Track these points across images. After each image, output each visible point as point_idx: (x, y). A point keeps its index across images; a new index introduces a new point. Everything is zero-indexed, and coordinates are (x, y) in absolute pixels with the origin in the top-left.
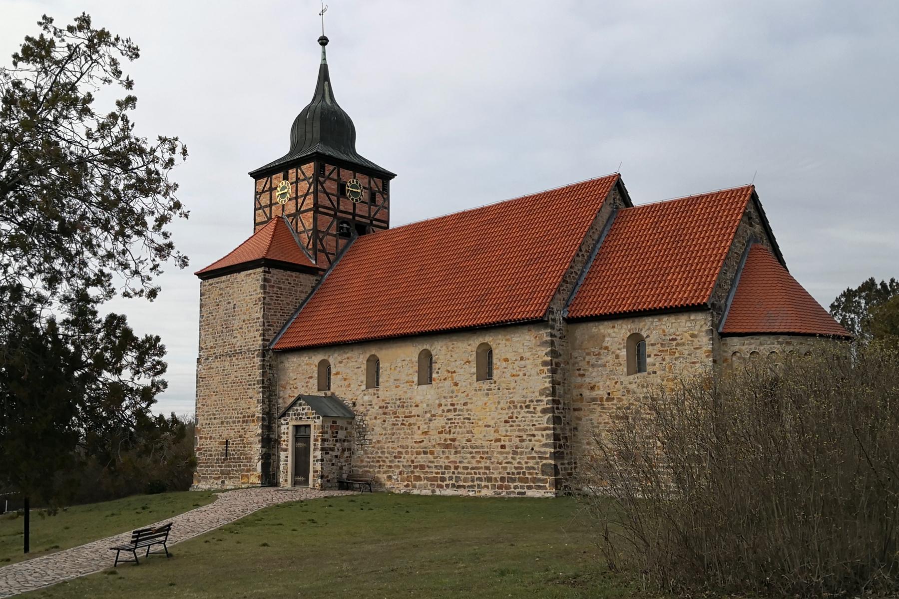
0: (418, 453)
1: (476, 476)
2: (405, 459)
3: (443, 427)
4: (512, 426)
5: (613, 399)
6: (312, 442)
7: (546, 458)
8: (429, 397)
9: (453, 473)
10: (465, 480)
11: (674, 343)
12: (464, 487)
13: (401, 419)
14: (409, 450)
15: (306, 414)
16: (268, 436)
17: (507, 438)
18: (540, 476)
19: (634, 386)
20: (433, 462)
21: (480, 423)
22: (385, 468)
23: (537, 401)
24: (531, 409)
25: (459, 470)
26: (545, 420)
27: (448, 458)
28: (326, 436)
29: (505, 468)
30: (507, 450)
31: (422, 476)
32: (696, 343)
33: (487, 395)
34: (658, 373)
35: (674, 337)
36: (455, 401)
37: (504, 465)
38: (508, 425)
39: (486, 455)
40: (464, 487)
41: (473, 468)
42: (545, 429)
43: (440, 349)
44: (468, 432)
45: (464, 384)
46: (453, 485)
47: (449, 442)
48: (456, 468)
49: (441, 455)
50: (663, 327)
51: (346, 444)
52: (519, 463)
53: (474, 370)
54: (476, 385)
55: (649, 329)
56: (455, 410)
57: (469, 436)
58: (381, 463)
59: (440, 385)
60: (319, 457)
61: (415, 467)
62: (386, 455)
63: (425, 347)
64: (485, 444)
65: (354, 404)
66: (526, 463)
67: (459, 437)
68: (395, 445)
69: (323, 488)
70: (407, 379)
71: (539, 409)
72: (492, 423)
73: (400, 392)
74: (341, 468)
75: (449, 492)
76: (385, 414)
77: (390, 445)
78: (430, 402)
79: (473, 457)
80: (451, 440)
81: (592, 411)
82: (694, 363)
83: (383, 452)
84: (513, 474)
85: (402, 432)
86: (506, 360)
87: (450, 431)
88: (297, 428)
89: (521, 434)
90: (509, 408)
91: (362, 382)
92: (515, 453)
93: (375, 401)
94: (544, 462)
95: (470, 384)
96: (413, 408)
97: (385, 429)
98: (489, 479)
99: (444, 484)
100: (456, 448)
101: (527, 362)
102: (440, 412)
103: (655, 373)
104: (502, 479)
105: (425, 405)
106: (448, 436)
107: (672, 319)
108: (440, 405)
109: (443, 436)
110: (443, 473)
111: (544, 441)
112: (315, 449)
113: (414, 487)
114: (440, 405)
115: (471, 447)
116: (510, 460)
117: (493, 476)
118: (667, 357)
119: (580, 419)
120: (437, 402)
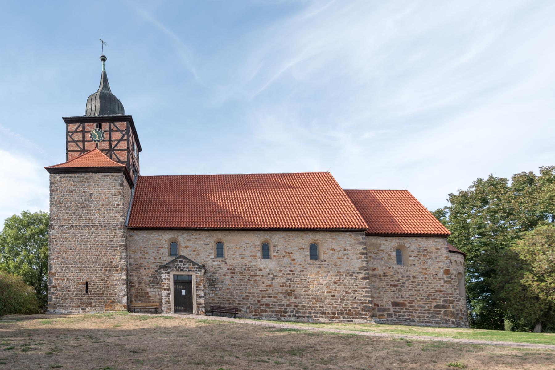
2: (251, 300)
3: (283, 283)
8: (272, 266)
9: (294, 309)
11: (426, 251)
12: (304, 317)
13: (247, 277)
14: (255, 295)
25: (299, 307)
27: (289, 300)
31: (268, 310)
38: (336, 285)
42: (364, 288)
43: (277, 239)
45: (300, 260)
46: (294, 316)
47: (289, 292)
48: (297, 306)
49: (283, 299)
56: (294, 274)
58: (231, 302)
61: (262, 305)
62: (235, 297)
63: (266, 237)
67: (298, 289)
70: (251, 254)
73: (245, 261)
76: (232, 273)
77: (239, 291)
89: (347, 290)
90: (337, 275)
93: (223, 265)
95: (305, 260)
97: (233, 282)
99: (287, 315)
103: (414, 265)
105: (268, 270)
109: (284, 288)
110: (286, 309)
114: (281, 271)
118: (421, 258)
120: (278, 269)
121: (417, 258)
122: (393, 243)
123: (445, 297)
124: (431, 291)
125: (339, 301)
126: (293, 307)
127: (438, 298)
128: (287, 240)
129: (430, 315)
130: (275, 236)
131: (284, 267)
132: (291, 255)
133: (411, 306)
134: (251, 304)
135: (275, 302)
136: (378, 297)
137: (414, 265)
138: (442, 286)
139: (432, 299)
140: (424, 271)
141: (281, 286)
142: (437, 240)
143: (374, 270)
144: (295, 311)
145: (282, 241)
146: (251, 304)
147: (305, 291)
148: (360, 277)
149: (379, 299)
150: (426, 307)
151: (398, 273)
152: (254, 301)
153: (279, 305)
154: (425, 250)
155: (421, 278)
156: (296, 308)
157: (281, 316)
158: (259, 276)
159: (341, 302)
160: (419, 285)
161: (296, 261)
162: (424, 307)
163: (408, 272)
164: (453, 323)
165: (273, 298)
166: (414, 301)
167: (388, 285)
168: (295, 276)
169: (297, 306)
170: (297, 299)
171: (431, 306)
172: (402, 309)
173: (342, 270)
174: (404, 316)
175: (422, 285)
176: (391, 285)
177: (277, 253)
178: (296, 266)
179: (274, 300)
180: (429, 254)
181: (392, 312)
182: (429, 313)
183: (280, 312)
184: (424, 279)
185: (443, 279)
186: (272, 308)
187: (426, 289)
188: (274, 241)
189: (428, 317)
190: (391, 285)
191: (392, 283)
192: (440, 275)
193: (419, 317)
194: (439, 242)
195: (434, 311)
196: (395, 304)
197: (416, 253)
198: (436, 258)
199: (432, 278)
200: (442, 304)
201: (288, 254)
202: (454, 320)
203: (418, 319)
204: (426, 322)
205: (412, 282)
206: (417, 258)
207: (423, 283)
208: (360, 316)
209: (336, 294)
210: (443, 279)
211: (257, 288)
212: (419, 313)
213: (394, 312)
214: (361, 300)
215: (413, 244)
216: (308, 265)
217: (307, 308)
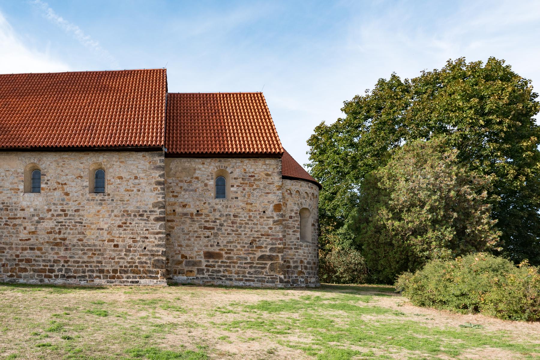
0: (24, 249)
1: (87, 269)
3: (52, 228)
7: (158, 255)
8: (37, 203)
9: (63, 266)
11: (253, 179)
12: (75, 277)
13: (4, 220)
14: (14, 246)
19: (220, 207)
20: (41, 257)
21: (93, 226)
25: (69, 263)
27: (57, 253)
31: (28, 268)
32: (270, 180)
34: (239, 198)
35: (253, 174)
36: (65, 207)
37: (116, 260)
38: (121, 229)
39: (97, 251)
40: (75, 277)
41: (84, 262)
42: (158, 233)
43: (49, 164)
44: (79, 233)
45: (75, 194)
46: (63, 276)
47: (59, 241)
50: (244, 167)
52: (132, 258)
53: (87, 184)
54: (88, 195)
55: (233, 167)
57: (81, 236)
59: (49, 193)
61: (21, 261)
63: (32, 161)
64: (97, 243)
66: (139, 259)
67: (70, 237)
70: (11, 186)
72: (105, 227)
78: (38, 207)
79: (84, 254)
80: (60, 239)
81: (184, 223)
82: (268, 193)
85: (5, 231)
89: (134, 236)
90: (123, 215)
95: (82, 195)
96: (19, 211)
98: (101, 271)
99: (53, 275)
103: (237, 198)
105: (32, 210)
106: (57, 236)
107: (252, 161)
109: (52, 236)
110: (53, 266)
111: (157, 242)
113: (20, 277)
116: (123, 256)
117: (105, 269)
118: (246, 188)
119: (173, 228)
120: (46, 207)
121: (241, 189)
122: (211, 167)
124: (255, 236)
125: (123, 254)
126: (62, 263)
127: (263, 246)
128: (61, 164)
129: (252, 270)
130: (45, 159)
131: (54, 204)
132: (65, 186)
133: (229, 258)
134: (6, 259)
135: (38, 257)
136: (187, 246)
137: (237, 198)
138: (271, 228)
139: (257, 247)
140: (249, 207)
141: (48, 233)
142: (268, 161)
143: (184, 206)
144: (64, 268)
145: (53, 166)
146: (6, 259)
147: (80, 240)
148: (152, 217)
149: (188, 248)
150: (248, 258)
151: (215, 210)
152: (12, 255)
153: (44, 261)
154: (252, 176)
155: (243, 216)
156: (66, 265)
157: (46, 276)
158: (20, 218)
159: (125, 255)
160: (241, 227)
161: (71, 195)
162: (246, 259)
163: (228, 209)
164: (281, 281)
165: (36, 251)
166: (232, 250)
167: (200, 228)
168: (68, 217)
169: (67, 262)
170: (68, 252)
171: (255, 257)
172: (217, 262)
173: (130, 208)
174: (219, 271)
175: (245, 227)
176: (206, 228)
177: (47, 183)
178: (71, 203)
179: (38, 253)
180: (256, 182)
181: (204, 267)
182: (251, 267)
183: (44, 271)
184: (248, 218)
185: (273, 217)
187: (249, 233)
188: (44, 166)
189: (249, 273)
190: (206, 228)
191: (207, 225)
192: (269, 213)
193: (237, 273)
194: (270, 165)
195: (257, 264)
196: (209, 255)
197: (240, 180)
198: (265, 188)
199: (258, 217)
200: (268, 253)
201: (60, 186)
202: (282, 276)
203: (236, 276)
204: (246, 280)
205: (233, 223)
206: (241, 189)
207: (246, 224)
208: (150, 274)
209: (120, 243)
210: (273, 217)
211: (17, 237)
212: (238, 267)
213: (206, 266)
214: (152, 251)
215: (236, 169)
216: (86, 202)
217: (80, 264)
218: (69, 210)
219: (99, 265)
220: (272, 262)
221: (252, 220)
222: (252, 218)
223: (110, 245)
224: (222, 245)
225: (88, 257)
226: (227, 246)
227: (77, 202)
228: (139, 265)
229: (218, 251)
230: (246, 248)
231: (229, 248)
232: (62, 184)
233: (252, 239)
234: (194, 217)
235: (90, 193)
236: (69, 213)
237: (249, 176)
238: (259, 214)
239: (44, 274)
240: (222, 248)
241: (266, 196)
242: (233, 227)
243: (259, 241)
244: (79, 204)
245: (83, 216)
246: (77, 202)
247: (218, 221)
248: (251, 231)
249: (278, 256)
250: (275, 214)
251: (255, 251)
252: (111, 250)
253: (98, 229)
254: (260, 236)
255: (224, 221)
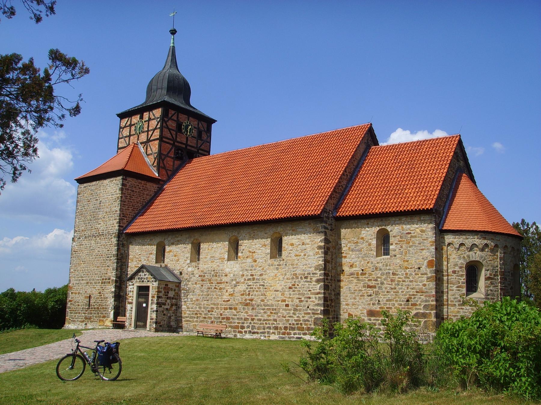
1: (266, 326)
2: (215, 314)
3: (244, 291)
4: (294, 291)
5: (366, 274)
6: (150, 298)
7: (317, 314)
8: (235, 269)
9: (250, 323)
10: (259, 328)
11: (409, 236)
13: (214, 285)
15: (147, 278)
16: (119, 293)
17: (290, 299)
18: (313, 326)
20: (236, 315)
21: (271, 288)
22: (201, 319)
23: (313, 274)
24: (309, 280)
25: (255, 321)
26: (318, 287)
27: (247, 312)
28: (161, 295)
29: (288, 320)
30: (290, 308)
31: (228, 325)
33: (277, 269)
36: (253, 272)
39: (274, 311)
40: (258, 333)
41: (264, 320)
46: (250, 332)
47: (248, 301)
48: (253, 320)
49: (242, 311)
51: (174, 300)
52: (298, 317)
54: (270, 261)
56: (254, 279)
58: (199, 315)
59: (244, 261)
60: (155, 309)
61: (223, 318)
62: (202, 309)
64: (274, 303)
65: (181, 273)
66: (303, 317)
68: (210, 302)
69: (157, 330)
71: (314, 279)
72: (280, 288)
74: (170, 317)
75: (248, 336)
76: (203, 280)
78: (236, 273)
79: (265, 312)
80: (249, 300)
81: (350, 282)
82: (422, 249)
83: (200, 308)
84: (293, 324)
85: (214, 293)
86: (292, 245)
87: (249, 294)
88: (140, 288)
90: (293, 278)
91: (187, 258)
92: (295, 310)
93: (196, 271)
94: (316, 316)
97: (202, 291)
98: (276, 328)
99: (243, 331)
100: (253, 306)
101: (307, 246)
102: (243, 280)
104: (286, 328)
105: (232, 275)
108: (243, 275)
109: (245, 297)
110: (243, 323)
112: (152, 303)
114: (243, 275)
115: (264, 305)
117: (279, 326)
118: (404, 246)
120: (241, 273)
121: (399, 246)
123: (426, 301)
124: (411, 293)
127: (418, 303)
130: (242, 231)
137: (395, 256)
138: (424, 285)
141: (242, 295)
149: (353, 307)
158: (224, 283)
160: (398, 285)
163: (388, 268)
165: (233, 311)
167: (364, 287)
170: (254, 311)
177: (242, 253)
183: (237, 327)
185: (426, 274)
186: (231, 322)
191: (370, 283)
199: (414, 274)
200: (422, 311)
205: (392, 281)
206: (399, 246)
218: (256, 275)
219: (275, 323)
220: (426, 320)
221: (408, 278)
222: (408, 276)
223: (283, 305)
224: (381, 303)
225: (268, 315)
226: (387, 304)
227: (262, 268)
228: (303, 323)
229: (378, 309)
230: (403, 306)
231: (388, 306)
232: (252, 253)
233: (408, 296)
234: (360, 276)
235: (271, 258)
236: (256, 277)
237: (407, 234)
238: (415, 271)
239: (237, 330)
240: (382, 306)
241: (421, 253)
242: (392, 284)
243: (415, 298)
244: (263, 269)
245: (265, 279)
246: (262, 268)
247: (379, 280)
248: (408, 288)
249: (430, 313)
250: (428, 270)
251: (410, 308)
252: (283, 309)
253: (275, 291)
254: (415, 294)
255: (384, 279)
